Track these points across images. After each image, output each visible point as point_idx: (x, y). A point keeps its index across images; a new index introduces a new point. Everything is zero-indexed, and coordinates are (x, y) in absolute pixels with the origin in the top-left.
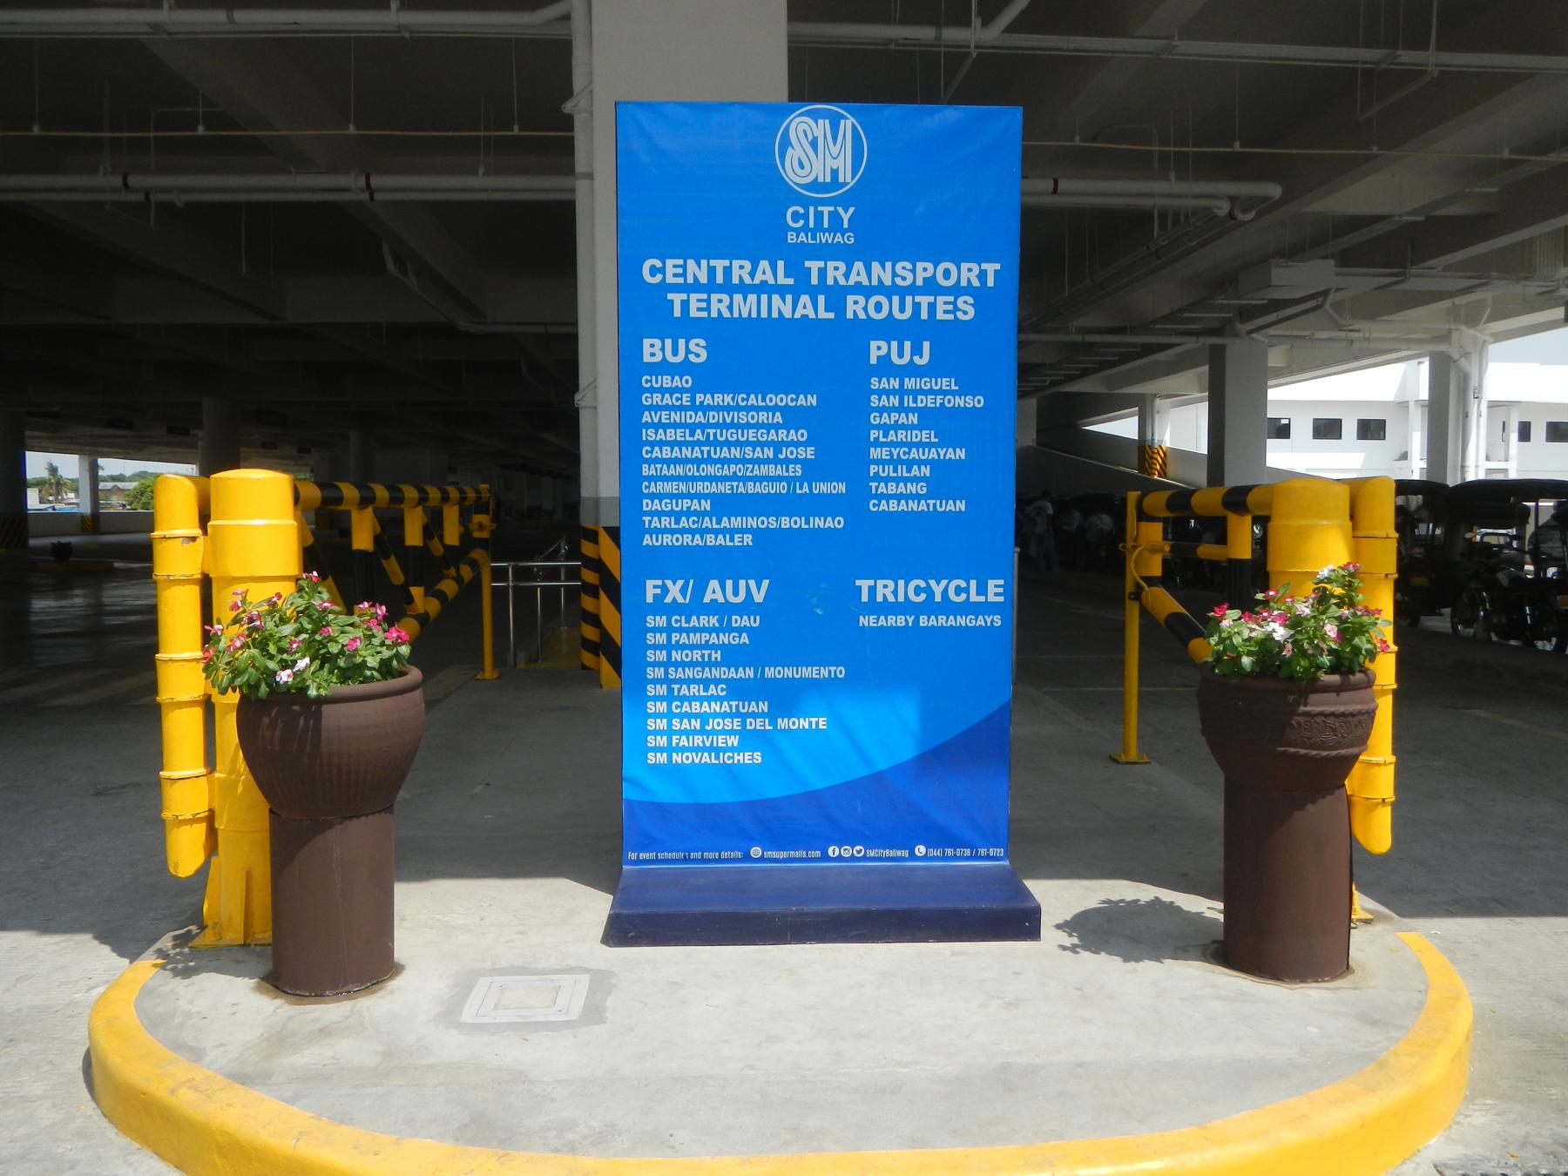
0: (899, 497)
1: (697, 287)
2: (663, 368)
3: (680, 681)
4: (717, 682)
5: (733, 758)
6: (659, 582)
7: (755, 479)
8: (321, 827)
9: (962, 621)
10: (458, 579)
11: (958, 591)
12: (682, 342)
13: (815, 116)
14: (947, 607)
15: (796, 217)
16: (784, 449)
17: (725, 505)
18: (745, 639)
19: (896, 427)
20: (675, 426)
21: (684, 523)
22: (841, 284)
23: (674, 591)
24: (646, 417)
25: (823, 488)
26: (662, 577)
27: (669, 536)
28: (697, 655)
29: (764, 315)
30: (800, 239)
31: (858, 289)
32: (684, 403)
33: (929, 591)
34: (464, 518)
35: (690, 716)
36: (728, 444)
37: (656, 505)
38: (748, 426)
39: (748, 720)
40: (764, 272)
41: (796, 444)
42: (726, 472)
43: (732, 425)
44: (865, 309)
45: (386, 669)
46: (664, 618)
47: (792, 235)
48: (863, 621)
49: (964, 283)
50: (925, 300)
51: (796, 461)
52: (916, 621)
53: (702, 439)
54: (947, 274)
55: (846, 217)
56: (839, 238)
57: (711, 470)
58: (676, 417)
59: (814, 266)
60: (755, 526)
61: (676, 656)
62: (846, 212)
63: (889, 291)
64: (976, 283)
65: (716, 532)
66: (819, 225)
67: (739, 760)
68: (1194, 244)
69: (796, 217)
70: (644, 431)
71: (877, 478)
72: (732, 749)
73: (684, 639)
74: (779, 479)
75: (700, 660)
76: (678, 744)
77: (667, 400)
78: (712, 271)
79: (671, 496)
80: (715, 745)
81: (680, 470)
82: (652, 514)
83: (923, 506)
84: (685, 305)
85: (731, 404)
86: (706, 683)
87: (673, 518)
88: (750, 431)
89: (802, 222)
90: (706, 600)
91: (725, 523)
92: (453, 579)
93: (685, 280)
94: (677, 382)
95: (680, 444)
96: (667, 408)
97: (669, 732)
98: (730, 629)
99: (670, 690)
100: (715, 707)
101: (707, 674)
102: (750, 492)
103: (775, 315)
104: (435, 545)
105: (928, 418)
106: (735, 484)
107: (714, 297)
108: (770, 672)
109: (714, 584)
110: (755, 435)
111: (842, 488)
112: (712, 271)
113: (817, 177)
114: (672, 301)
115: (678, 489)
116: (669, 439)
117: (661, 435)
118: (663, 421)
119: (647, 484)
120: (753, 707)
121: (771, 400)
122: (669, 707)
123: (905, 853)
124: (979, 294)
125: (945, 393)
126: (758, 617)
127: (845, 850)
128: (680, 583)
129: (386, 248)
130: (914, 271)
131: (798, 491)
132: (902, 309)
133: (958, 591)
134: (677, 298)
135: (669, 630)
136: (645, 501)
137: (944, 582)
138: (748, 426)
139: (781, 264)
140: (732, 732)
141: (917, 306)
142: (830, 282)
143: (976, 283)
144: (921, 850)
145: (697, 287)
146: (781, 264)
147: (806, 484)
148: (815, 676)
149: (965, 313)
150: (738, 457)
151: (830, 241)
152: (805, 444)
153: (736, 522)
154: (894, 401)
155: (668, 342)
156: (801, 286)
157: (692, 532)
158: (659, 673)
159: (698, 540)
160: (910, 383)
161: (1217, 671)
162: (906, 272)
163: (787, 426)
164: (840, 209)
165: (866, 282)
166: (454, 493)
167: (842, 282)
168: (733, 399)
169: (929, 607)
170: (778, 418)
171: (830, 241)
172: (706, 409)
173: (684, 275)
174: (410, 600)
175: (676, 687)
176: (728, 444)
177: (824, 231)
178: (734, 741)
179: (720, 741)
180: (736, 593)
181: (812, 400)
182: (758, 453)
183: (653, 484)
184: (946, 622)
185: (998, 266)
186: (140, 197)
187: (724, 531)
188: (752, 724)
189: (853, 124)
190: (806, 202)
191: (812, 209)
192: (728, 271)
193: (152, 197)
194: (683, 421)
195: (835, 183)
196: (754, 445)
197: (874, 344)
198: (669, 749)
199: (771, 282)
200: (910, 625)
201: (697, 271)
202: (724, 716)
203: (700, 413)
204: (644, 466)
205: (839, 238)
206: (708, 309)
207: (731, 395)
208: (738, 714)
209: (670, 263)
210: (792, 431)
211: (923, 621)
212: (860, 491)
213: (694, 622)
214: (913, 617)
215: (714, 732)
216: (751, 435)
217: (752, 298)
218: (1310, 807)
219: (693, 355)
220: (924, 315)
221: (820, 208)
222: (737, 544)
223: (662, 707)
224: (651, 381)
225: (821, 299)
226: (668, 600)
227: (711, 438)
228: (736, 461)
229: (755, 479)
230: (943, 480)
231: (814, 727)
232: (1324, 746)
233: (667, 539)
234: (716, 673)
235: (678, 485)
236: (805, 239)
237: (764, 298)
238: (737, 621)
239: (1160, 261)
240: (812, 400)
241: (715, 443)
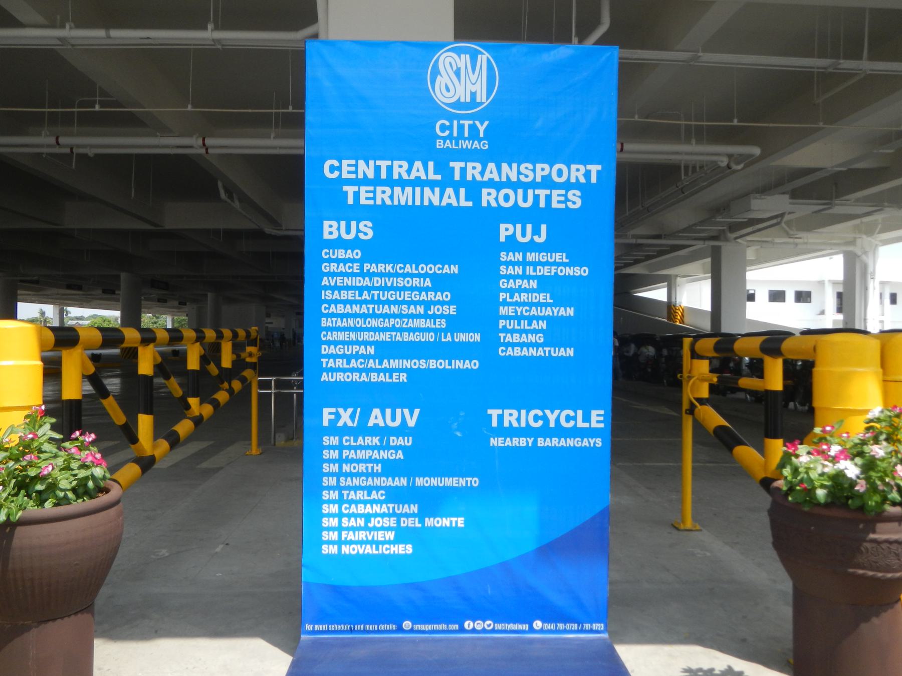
0: (522, 345)
1: (366, 181)
2: (339, 243)
3: (349, 488)
4: (378, 488)
5: (390, 549)
6: (333, 410)
7: (410, 330)
8: (19, 631)
9: (571, 442)
10: (231, 391)
11: (568, 418)
12: (353, 224)
13: (459, 51)
14: (560, 432)
15: (443, 128)
16: (432, 307)
17: (385, 350)
18: (400, 455)
19: (520, 290)
20: (347, 288)
21: (353, 363)
22: (477, 180)
23: (345, 417)
24: (325, 281)
25: (462, 337)
26: (336, 406)
27: (342, 374)
28: (362, 467)
29: (418, 203)
30: (446, 145)
31: (491, 184)
32: (355, 271)
33: (545, 418)
34: (237, 348)
35: (356, 516)
36: (389, 302)
37: (332, 350)
38: (404, 289)
39: (402, 519)
42: (387, 325)
43: (392, 288)
44: (496, 199)
45: (81, 490)
46: (337, 438)
47: (440, 142)
48: (493, 442)
49: (573, 180)
50: (542, 193)
51: (442, 316)
52: (535, 442)
53: (368, 299)
55: (482, 129)
57: (375, 323)
58: (348, 281)
59: (457, 166)
60: (409, 367)
61: (346, 468)
62: (482, 125)
64: (582, 180)
65: (378, 371)
67: (394, 551)
68: (705, 184)
70: (323, 292)
71: (505, 330)
72: (389, 542)
73: (352, 455)
74: (428, 330)
75: (365, 471)
76: (346, 538)
77: (342, 268)
78: (377, 169)
79: (343, 343)
80: (376, 539)
81: (351, 323)
82: (329, 356)
83: (540, 352)
84: (357, 195)
85: (392, 271)
86: (369, 489)
87: (345, 360)
88: (406, 293)
89: (447, 133)
90: (370, 424)
91: (385, 364)
92: (226, 390)
93: (357, 176)
94: (349, 254)
95: (351, 303)
96: (341, 274)
97: (340, 529)
98: (388, 447)
99: (341, 495)
100: (376, 508)
101: (370, 482)
102: (405, 340)
103: (426, 203)
104: (213, 369)
105: (544, 283)
106: (394, 334)
107: (379, 189)
108: (420, 481)
109: (376, 412)
110: (410, 296)
111: (477, 337)
112: (377, 169)
113: (460, 98)
114: (346, 192)
115: (349, 338)
116: (342, 298)
117: (336, 295)
118: (338, 284)
119: (325, 334)
120: (406, 509)
121: (422, 269)
122: (340, 508)
123: (525, 627)
124: (585, 189)
125: (558, 264)
126: (411, 438)
127: (478, 624)
128: (350, 410)
129: (220, 184)
130: (534, 171)
131: (443, 340)
132: (525, 200)
133: (568, 418)
134: (350, 190)
135: (341, 447)
136: (323, 347)
137: (557, 412)
138: (404, 289)
139: (431, 165)
140: (389, 529)
141: (536, 198)
142: (469, 178)
143: (582, 180)
144: (538, 624)
145: (366, 181)
146: (431, 165)
147: (449, 334)
148: (455, 485)
149: (574, 203)
150: (396, 312)
151: (469, 147)
152: (449, 303)
153: (394, 363)
154: (519, 270)
155: (343, 223)
157: (360, 371)
158: (333, 481)
159: (364, 378)
160: (531, 257)
161: (790, 499)
162: (528, 172)
163: (435, 289)
164: (477, 123)
165: (497, 179)
166: (227, 333)
167: (479, 178)
168: (393, 268)
169: (546, 431)
170: (428, 283)
171: (469, 147)
172: (371, 275)
173: (356, 172)
174: (188, 407)
175: (345, 492)
176: (389, 302)
177: (465, 139)
178: (391, 535)
179: (380, 535)
180: (393, 419)
181: (455, 269)
182: (412, 310)
183: (329, 333)
184: (559, 443)
185: (599, 167)
186: (68, 151)
187: (385, 371)
188: (405, 522)
189: (488, 58)
190: (451, 117)
191: (455, 122)
192: (390, 169)
193: (74, 150)
194: (354, 285)
195: (473, 103)
196: (409, 303)
197: (503, 226)
198: (340, 543)
199: (424, 177)
200: (530, 445)
201: (366, 169)
202: (383, 515)
203: (367, 279)
204: (323, 319)
206: (374, 198)
207: (392, 265)
208: (394, 514)
209: (345, 163)
210: (439, 293)
211: (541, 442)
212: (491, 342)
213: (360, 441)
214: (532, 439)
215: (375, 529)
216: (406, 295)
217: (409, 190)
218: (875, 620)
219: (362, 234)
220: (542, 204)
221: (462, 122)
222: (394, 380)
223: (334, 508)
224: (329, 253)
225: (462, 191)
226: (340, 424)
227: (376, 298)
228: (394, 316)
229: (410, 330)
231: (469, 485)
232: (889, 569)
233: (340, 376)
234: (377, 481)
235: (349, 334)
236: (450, 145)
237: (418, 190)
238: (394, 441)
239: (683, 195)
240: (455, 269)
241: (379, 302)
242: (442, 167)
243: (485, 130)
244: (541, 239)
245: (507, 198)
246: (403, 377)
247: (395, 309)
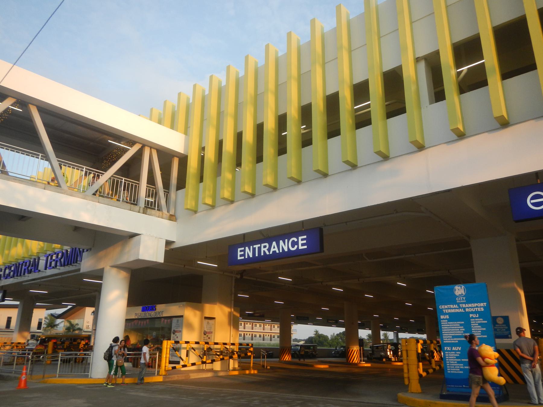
1: (446, 309)
2: (444, 319)
3: (451, 361)
7: (457, 333)
12: (445, 316)
15: (458, 299)
18: (459, 355)
20: (446, 327)
23: (449, 349)
28: (452, 357)
31: (467, 308)
40: (455, 306)
44: (468, 310)
50: (476, 308)
54: (479, 305)
56: (464, 301)
58: (446, 325)
59: (461, 305)
61: (450, 357)
63: (471, 308)
66: (461, 300)
74: (461, 333)
78: (448, 306)
79: (447, 336)
81: (447, 332)
84: (445, 311)
86: (454, 361)
98: (456, 354)
100: (456, 365)
105: (480, 324)
107: (449, 310)
108: (463, 360)
112: (448, 306)
124: (484, 307)
130: (474, 305)
132: (473, 310)
134: (444, 310)
135: (448, 354)
141: (475, 309)
142: (463, 307)
143: (483, 306)
145: (446, 309)
146: (457, 305)
153: (455, 339)
154: (474, 322)
155: (444, 316)
156: (460, 308)
160: (476, 320)
178: (459, 370)
179: (457, 370)
180: (457, 349)
185: (486, 303)
188: (461, 367)
192: (450, 306)
195: (462, 294)
197: (470, 315)
198: (451, 371)
201: (446, 307)
216: (456, 327)
225: (462, 309)
226: (448, 350)
230: (483, 333)
238: (457, 353)
240: (463, 323)
241: (451, 329)
243: (465, 299)
245: (470, 310)
246: (457, 341)
247: (454, 330)
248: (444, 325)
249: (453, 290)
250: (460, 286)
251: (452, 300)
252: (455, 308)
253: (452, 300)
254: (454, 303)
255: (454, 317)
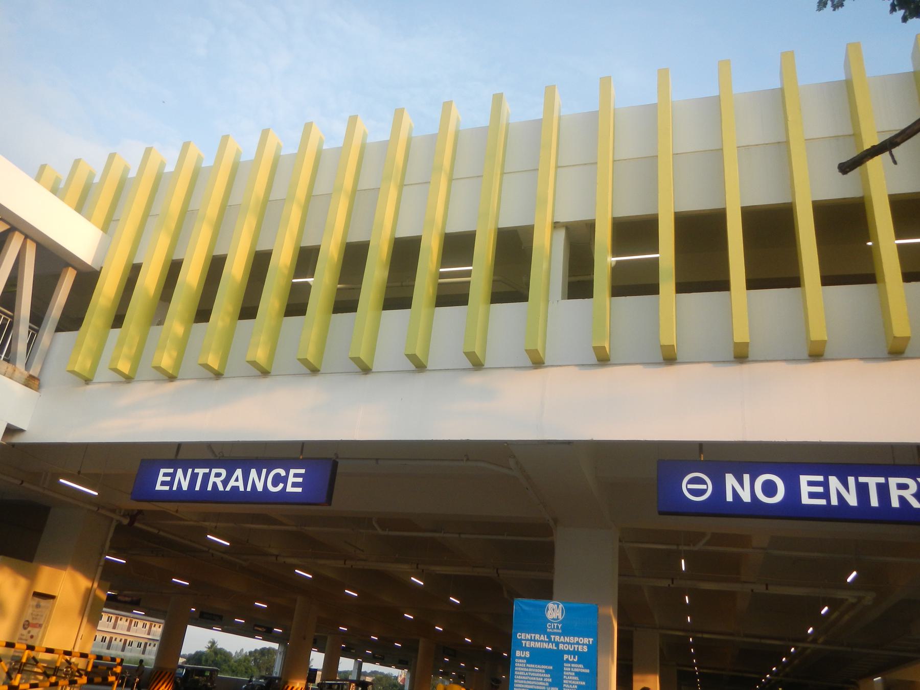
1: (528, 640)
2: (520, 658)
7: (539, 685)
12: (524, 652)
13: (554, 604)
15: (549, 626)
19: (570, 675)
20: (522, 671)
29: (542, 647)
31: (562, 642)
36: (533, 676)
40: (542, 638)
41: (548, 678)
50: (576, 646)
54: (581, 640)
56: (558, 631)
57: (529, 682)
58: (522, 669)
59: (553, 637)
63: (569, 643)
64: (588, 643)
69: (549, 626)
74: (544, 686)
77: (521, 665)
78: (531, 636)
81: (522, 682)
84: (525, 644)
95: (523, 676)
105: (577, 674)
107: (532, 642)
112: (531, 636)
124: (588, 646)
132: (571, 648)
139: (546, 636)
141: (574, 648)
142: (556, 640)
143: (588, 643)
145: (528, 640)
146: (546, 636)
152: (549, 678)
154: (569, 669)
155: (522, 652)
156: (550, 641)
160: (573, 665)
163: (546, 673)
165: (563, 641)
167: (558, 641)
170: (544, 671)
172: (528, 668)
190: (552, 622)
192: (535, 637)
195: (558, 619)
201: (528, 636)
205: (558, 631)
209: (523, 634)
216: (538, 675)
217: (539, 643)
220: (576, 650)
225: (554, 644)
228: (534, 681)
241: (530, 676)
242: (549, 637)
244: (576, 660)
247: (534, 679)
248: (520, 669)
249: (543, 609)
250: (557, 603)
251: (540, 625)
252: (542, 641)
253: (540, 625)
254: (542, 630)
255: (538, 656)
